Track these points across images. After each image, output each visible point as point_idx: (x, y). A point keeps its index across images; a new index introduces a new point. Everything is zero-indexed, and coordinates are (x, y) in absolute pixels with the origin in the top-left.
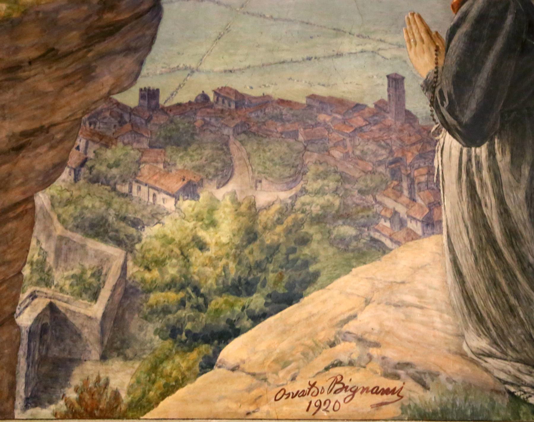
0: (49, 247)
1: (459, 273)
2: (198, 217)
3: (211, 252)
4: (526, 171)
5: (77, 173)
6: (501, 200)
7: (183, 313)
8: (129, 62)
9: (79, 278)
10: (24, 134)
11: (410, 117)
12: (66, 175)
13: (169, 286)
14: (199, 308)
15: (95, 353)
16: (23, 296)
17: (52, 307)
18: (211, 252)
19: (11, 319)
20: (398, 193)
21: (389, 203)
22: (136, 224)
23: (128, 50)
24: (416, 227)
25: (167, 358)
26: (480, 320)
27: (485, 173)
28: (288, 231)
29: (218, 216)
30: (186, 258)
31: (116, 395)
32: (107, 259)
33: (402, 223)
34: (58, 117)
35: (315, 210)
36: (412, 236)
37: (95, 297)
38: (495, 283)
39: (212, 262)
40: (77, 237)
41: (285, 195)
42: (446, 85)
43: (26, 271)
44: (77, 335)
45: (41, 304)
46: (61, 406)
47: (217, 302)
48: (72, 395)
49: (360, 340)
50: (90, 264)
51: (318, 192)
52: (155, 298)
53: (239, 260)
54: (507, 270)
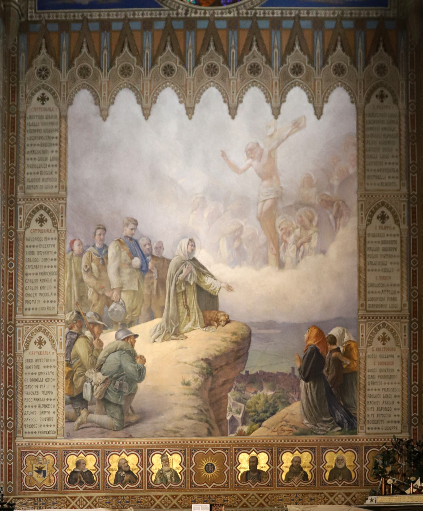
0: (231, 404)
1: (303, 408)
2: (257, 398)
3: (260, 405)
4: (316, 388)
5: (235, 389)
6: (311, 394)
7: (256, 417)
8: (243, 365)
9: (237, 410)
10: (225, 381)
11: (295, 376)
12: (233, 390)
14: (258, 416)
15: (241, 424)
16: (227, 414)
17: (233, 416)
18: (260, 405)
19: (226, 418)
20: (293, 393)
21: (291, 394)
22: (246, 399)
23: (243, 362)
24: (296, 399)
25: (253, 425)
26: (306, 417)
27: (309, 388)
28: (273, 401)
29: (261, 397)
30: (255, 406)
31: (245, 432)
32: (241, 407)
33: (294, 399)
34: (230, 377)
35: (278, 396)
36: (295, 401)
37: (240, 414)
38: (309, 410)
39: (260, 407)
40: (236, 402)
41: (272, 393)
42: (302, 369)
43: (228, 409)
44: (237, 421)
45: (230, 415)
46: (235, 434)
47: (261, 414)
48: (237, 432)
49: (286, 421)
50: (239, 408)
51: (279, 392)
52: (251, 414)
53: (265, 406)
54: (311, 408)
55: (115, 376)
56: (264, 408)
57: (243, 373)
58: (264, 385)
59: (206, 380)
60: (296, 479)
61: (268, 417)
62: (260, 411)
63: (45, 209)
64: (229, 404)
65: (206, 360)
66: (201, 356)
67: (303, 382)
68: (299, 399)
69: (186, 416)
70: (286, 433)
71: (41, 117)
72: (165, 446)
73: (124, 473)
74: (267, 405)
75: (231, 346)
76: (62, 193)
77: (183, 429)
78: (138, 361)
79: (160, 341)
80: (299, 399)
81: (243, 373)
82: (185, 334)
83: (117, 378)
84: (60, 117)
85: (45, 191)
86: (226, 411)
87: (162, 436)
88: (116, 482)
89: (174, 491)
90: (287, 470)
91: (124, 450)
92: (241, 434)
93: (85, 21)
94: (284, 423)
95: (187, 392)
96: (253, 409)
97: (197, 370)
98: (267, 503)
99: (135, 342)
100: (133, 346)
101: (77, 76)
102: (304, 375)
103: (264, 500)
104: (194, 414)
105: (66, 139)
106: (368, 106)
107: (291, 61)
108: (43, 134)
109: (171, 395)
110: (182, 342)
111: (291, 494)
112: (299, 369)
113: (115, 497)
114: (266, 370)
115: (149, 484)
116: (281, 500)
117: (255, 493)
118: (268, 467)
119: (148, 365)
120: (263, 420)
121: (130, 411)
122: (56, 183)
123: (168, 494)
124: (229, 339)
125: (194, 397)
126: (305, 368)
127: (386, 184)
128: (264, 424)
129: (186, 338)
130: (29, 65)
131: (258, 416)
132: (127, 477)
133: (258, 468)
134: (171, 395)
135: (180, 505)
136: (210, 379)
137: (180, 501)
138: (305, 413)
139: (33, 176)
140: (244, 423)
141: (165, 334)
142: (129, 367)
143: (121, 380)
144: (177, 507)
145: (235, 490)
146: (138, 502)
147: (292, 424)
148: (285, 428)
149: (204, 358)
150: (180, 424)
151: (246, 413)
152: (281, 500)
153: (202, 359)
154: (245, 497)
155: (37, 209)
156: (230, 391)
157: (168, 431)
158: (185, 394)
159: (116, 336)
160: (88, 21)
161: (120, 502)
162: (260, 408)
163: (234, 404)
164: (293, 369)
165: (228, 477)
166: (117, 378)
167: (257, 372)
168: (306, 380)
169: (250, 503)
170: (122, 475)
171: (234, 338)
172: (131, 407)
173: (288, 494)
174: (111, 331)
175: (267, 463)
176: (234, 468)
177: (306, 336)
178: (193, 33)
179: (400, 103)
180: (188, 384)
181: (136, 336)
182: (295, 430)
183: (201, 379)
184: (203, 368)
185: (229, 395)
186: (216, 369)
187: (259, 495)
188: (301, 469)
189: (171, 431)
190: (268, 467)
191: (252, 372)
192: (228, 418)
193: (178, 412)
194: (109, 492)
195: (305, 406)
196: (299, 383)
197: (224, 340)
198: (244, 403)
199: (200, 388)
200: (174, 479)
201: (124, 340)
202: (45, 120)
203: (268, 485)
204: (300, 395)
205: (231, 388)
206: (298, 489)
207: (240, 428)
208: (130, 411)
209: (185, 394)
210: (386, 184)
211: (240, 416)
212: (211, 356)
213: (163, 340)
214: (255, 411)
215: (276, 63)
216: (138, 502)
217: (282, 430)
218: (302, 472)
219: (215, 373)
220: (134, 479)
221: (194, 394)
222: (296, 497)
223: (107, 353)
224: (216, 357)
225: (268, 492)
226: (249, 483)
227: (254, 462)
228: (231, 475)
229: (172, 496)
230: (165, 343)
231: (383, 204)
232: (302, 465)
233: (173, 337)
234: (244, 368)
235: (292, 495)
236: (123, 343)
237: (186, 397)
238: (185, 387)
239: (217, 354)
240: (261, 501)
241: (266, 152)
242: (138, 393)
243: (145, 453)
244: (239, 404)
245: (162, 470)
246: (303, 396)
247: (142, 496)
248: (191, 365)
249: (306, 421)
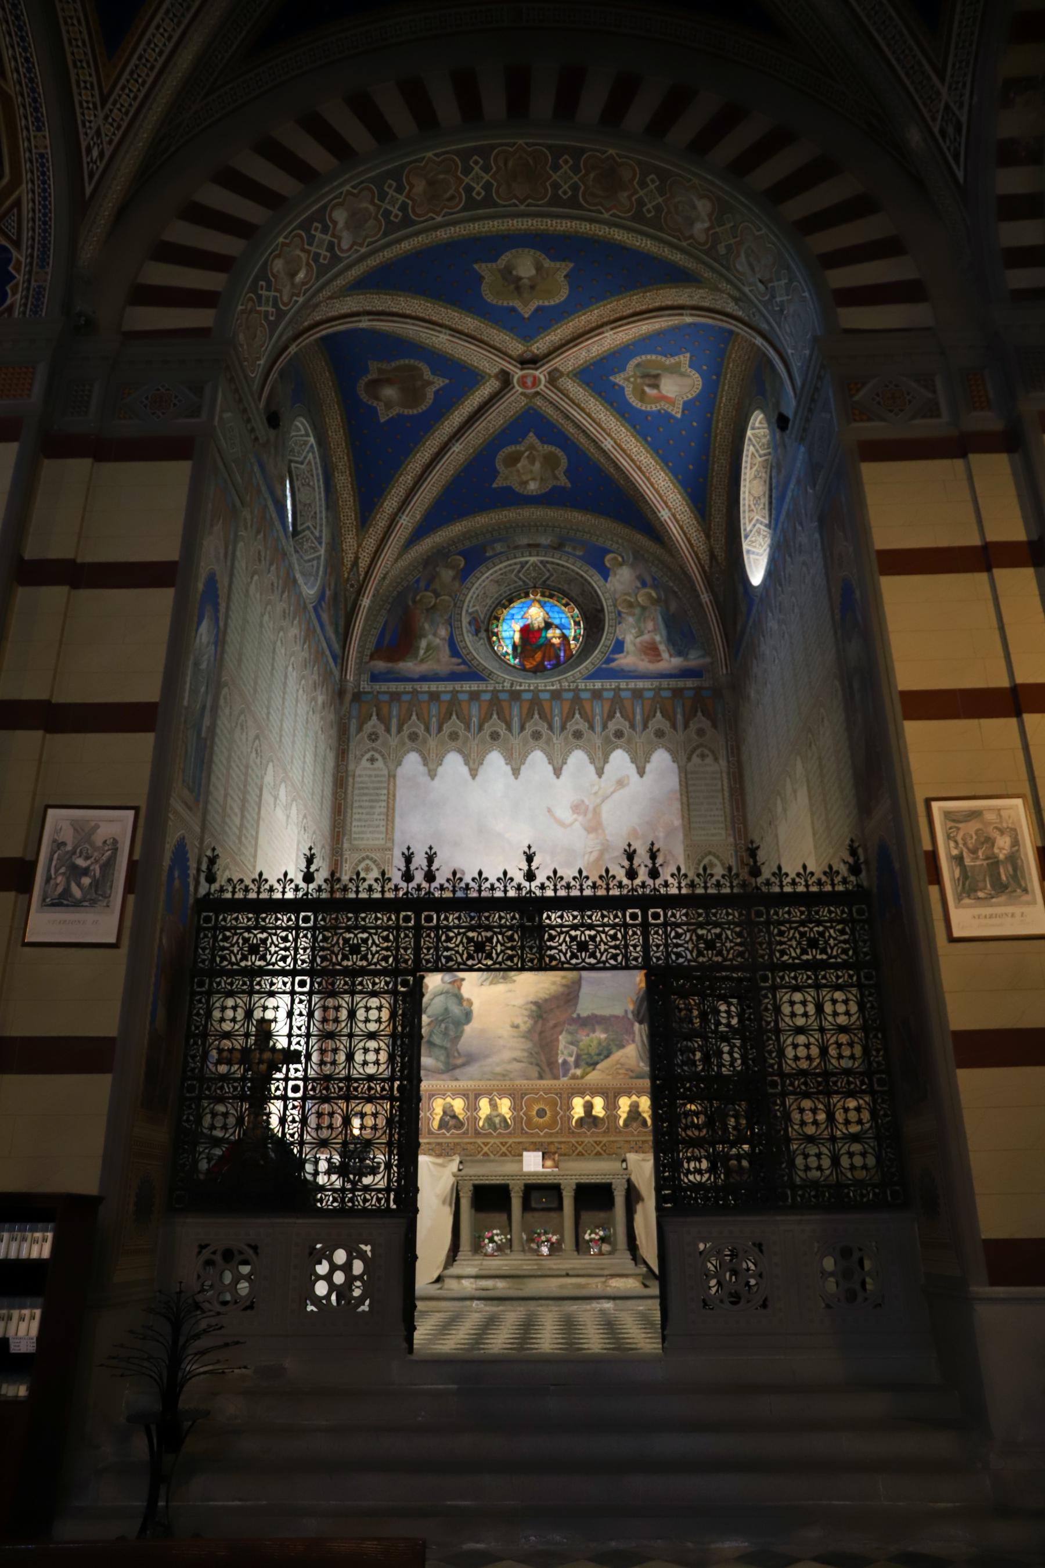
57: (575, 1016)
59: (536, 1023)
60: (635, 1125)
63: (371, 859)
64: (561, 1047)
65: (536, 1003)
66: (531, 998)
67: (637, 1025)
68: (633, 1041)
69: (515, 1060)
71: (370, 776)
75: (561, 989)
76: (389, 845)
78: (465, 1004)
81: (575, 1016)
83: (442, 1021)
84: (389, 776)
85: (372, 842)
86: (557, 1054)
88: (440, 1127)
90: (624, 1116)
92: (574, 1077)
93: (415, 693)
94: (619, 1066)
95: (516, 1034)
97: (526, 1013)
100: (459, 988)
101: (407, 740)
105: (394, 796)
106: (689, 764)
107: (612, 726)
108: (372, 791)
110: (510, 986)
112: (633, 1012)
113: (439, 1144)
114: (598, 1012)
115: (476, 1130)
119: (475, 1008)
120: (596, 1064)
121: (456, 1054)
122: (384, 836)
125: (523, 1040)
126: (639, 1012)
127: (713, 835)
128: (599, 1067)
130: (360, 729)
132: (452, 1122)
133: (594, 1113)
139: (359, 829)
140: (577, 1066)
142: (455, 1010)
148: (621, 1071)
150: (509, 1067)
151: (578, 1058)
155: (363, 859)
156: (561, 1033)
159: (442, 979)
160: (418, 692)
162: (593, 1050)
163: (565, 1047)
164: (626, 1011)
166: (442, 1021)
168: (641, 1022)
171: (564, 981)
172: (457, 1050)
178: (518, 703)
179: (721, 761)
180: (517, 1027)
182: (631, 1074)
183: (530, 1022)
184: (532, 1011)
185: (560, 1037)
188: (639, 1114)
190: (604, 1113)
191: (584, 1014)
192: (560, 1061)
193: (508, 1055)
196: (632, 1025)
197: (554, 983)
198: (577, 1046)
202: (373, 779)
203: (604, 1132)
206: (638, 1136)
207: (572, 1071)
208: (456, 1054)
210: (713, 835)
213: (491, 983)
214: (588, 1054)
215: (598, 728)
219: (545, 1016)
220: (460, 1124)
221: (523, 1037)
224: (546, 1000)
227: (589, 1107)
230: (493, 987)
231: (710, 853)
232: (640, 1109)
236: (449, 986)
239: (547, 997)
240: (598, 1149)
241: (591, 807)
243: (472, 1096)
244: (572, 1047)
246: (637, 1038)
249: (642, 1064)
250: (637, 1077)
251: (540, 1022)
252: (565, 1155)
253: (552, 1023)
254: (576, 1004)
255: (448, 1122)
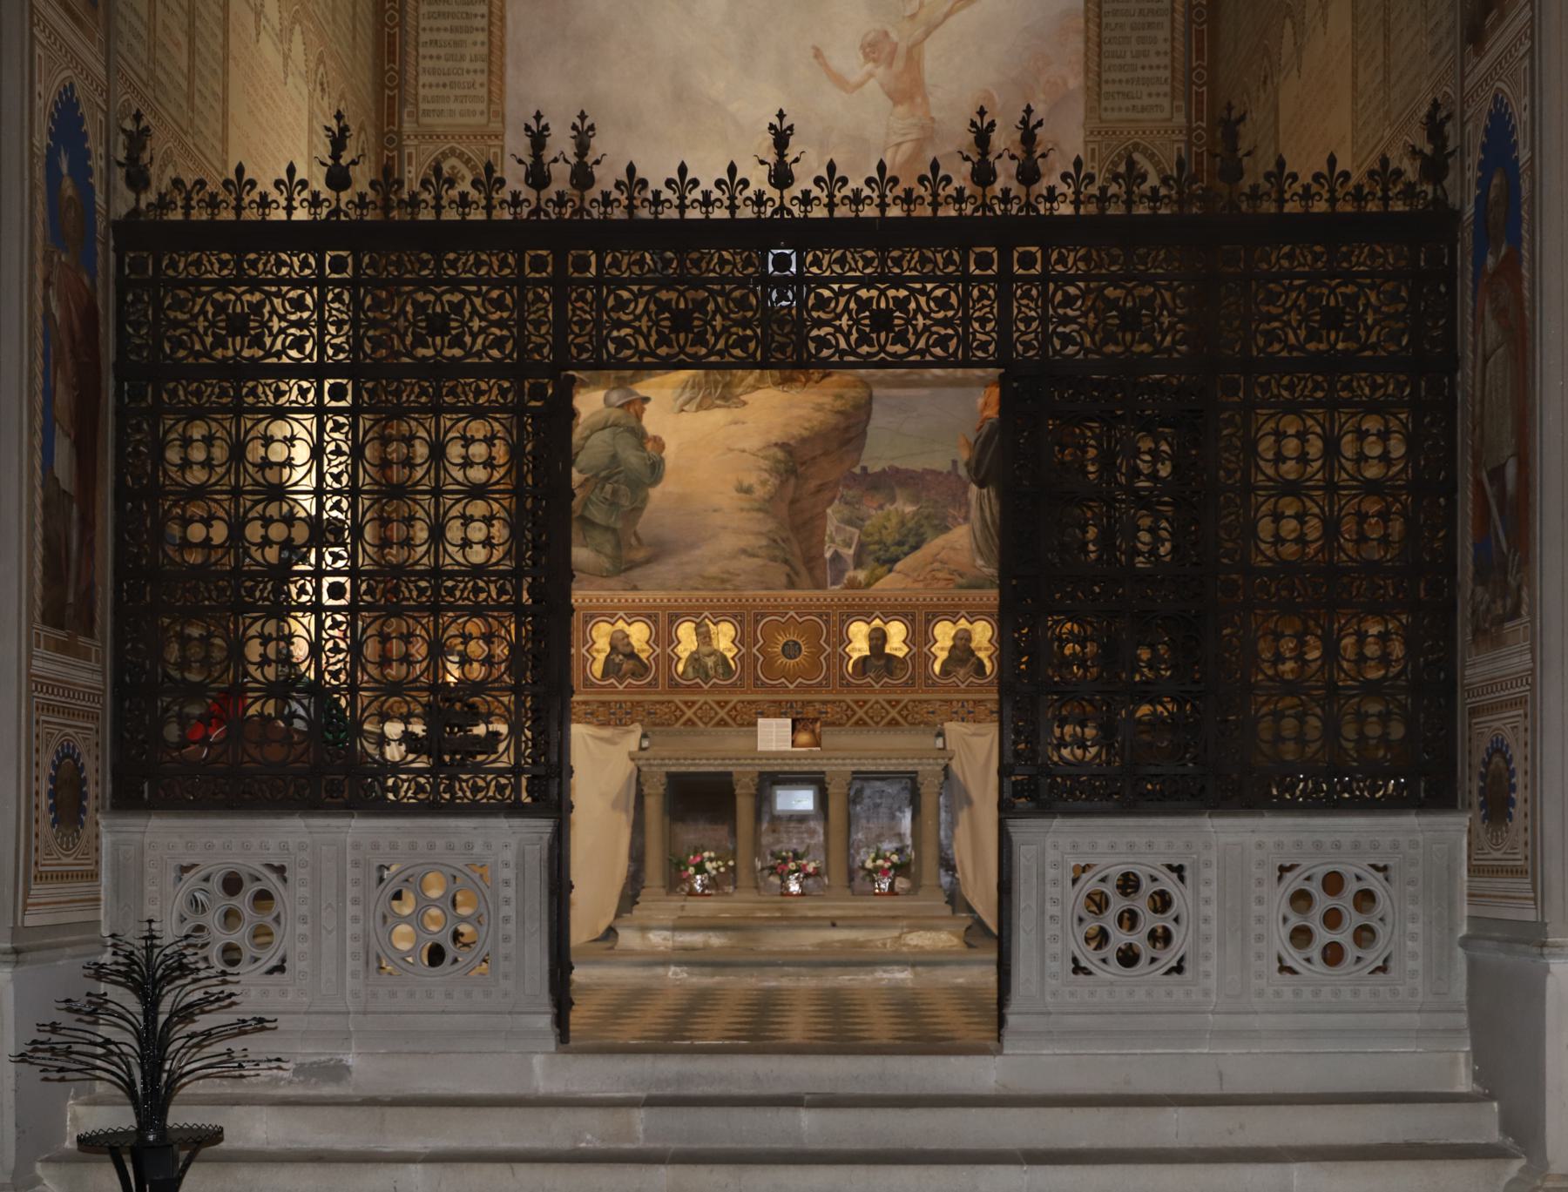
0: (833, 529)
9: (844, 541)
11: (959, 477)
12: (836, 502)
13: (876, 543)
19: (822, 555)
22: (863, 520)
24: (961, 520)
36: (959, 524)
38: (987, 540)
41: (914, 508)
42: (973, 464)
45: (832, 550)
47: (892, 549)
51: (927, 507)
52: (872, 547)
55: (603, 474)
56: (897, 537)
57: (857, 470)
58: (898, 491)
59: (783, 483)
60: (962, 672)
61: (906, 554)
62: (889, 541)
64: (830, 529)
65: (783, 446)
66: (774, 439)
67: (974, 488)
68: (966, 519)
69: (744, 551)
70: (942, 583)
72: (703, 608)
73: (621, 657)
74: (904, 531)
75: (832, 420)
77: (738, 575)
78: (649, 446)
79: (694, 408)
80: (966, 519)
81: (857, 470)
82: (743, 398)
83: (607, 479)
86: (822, 542)
87: (697, 589)
89: (721, 693)
90: (943, 655)
91: (621, 613)
92: (853, 585)
94: (937, 565)
95: (746, 505)
96: (876, 538)
98: (905, 718)
99: (643, 410)
100: (639, 418)
102: (976, 473)
103: (899, 713)
104: (760, 547)
109: (715, 511)
110: (737, 413)
111: (951, 701)
112: (967, 464)
113: (603, 703)
114: (901, 464)
115: (671, 679)
116: (933, 713)
117: (881, 698)
118: (906, 650)
119: (669, 454)
120: (896, 560)
121: (633, 541)
123: (710, 699)
124: (828, 407)
125: (761, 515)
126: (979, 462)
128: (898, 566)
129: (745, 403)
131: (887, 551)
132: (627, 666)
133: (887, 650)
134: (715, 511)
135: (734, 719)
136: (792, 481)
137: (734, 713)
138: (978, 547)
140: (859, 564)
141: (703, 397)
142: (632, 458)
143: (616, 482)
144: (726, 724)
145: (841, 692)
146: (650, 713)
147: (952, 567)
148: (940, 575)
149: (780, 442)
151: (862, 546)
152: (933, 713)
153: (776, 445)
154: (861, 707)
156: (830, 502)
157: (709, 578)
158: (742, 510)
159: (606, 400)
161: (614, 714)
163: (838, 529)
164: (955, 462)
165: (828, 669)
166: (607, 479)
167: (884, 470)
168: (981, 485)
169: (872, 718)
170: (617, 661)
171: (838, 404)
172: (635, 534)
173: (946, 701)
174: (595, 390)
175: (904, 642)
176: (840, 650)
177: (980, 401)
180: (748, 491)
181: (646, 400)
183: (773, 481)
184: (779, 461)
185: (829, 511)
186: (803, 464)
187: (889, 702)
188: (972, 653)
189: (714, 578)
190: (906, 650)
191: (875, 467)
192: (828, 555)
193: (729, 543)
194: (591, 693)
195: (978, 534)
197: (819, 408)
198: (859, 527)
199: (771, 498)
200: (721, 671)
201: (621, 406)
203: (906, 683)
204: (968, 512)
205: (833, 499)
206: (966, 692)
207: (850, 574)
208: (633, 541)
209: (742, 510)
211: (851, 552)
212: (793, 437)
213: (700, 407)
216: (650, 713)
217: (934, 578)
218: (973, 660)
219: (800, 470)
220: (641, 669)
221: (759, 510)
222: (963, 706)
223: (588, 432)
224: (804, 440)
225: (906, 698)
226: (869, 679)
228: (834, 663)
229: (718, 703)
230: (702, 414)
232: (973, 645)
233: (718, 402)
234: (858, 461)
235: (955, 703)
236: (619, 412)
237: (744, 514)
238: (742, 495)
239: (805, 433)
242: (650, 506)
243: (663, 619)
244: (849, 528)
245: (697, 652)
246: (974, 514)
247: (658, 702)
248: (754, 455)
249: (980, 562)
250: (970, 587)
251: (792, 481)
252: (833, 724)
253: (813, 484)
254: (860, 448)
255: (620, 665)
